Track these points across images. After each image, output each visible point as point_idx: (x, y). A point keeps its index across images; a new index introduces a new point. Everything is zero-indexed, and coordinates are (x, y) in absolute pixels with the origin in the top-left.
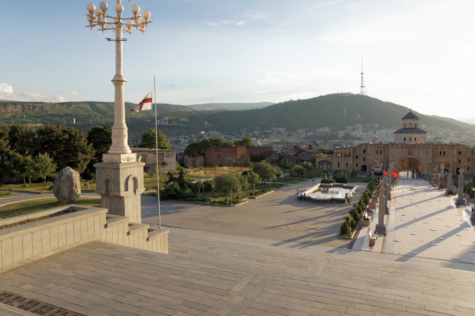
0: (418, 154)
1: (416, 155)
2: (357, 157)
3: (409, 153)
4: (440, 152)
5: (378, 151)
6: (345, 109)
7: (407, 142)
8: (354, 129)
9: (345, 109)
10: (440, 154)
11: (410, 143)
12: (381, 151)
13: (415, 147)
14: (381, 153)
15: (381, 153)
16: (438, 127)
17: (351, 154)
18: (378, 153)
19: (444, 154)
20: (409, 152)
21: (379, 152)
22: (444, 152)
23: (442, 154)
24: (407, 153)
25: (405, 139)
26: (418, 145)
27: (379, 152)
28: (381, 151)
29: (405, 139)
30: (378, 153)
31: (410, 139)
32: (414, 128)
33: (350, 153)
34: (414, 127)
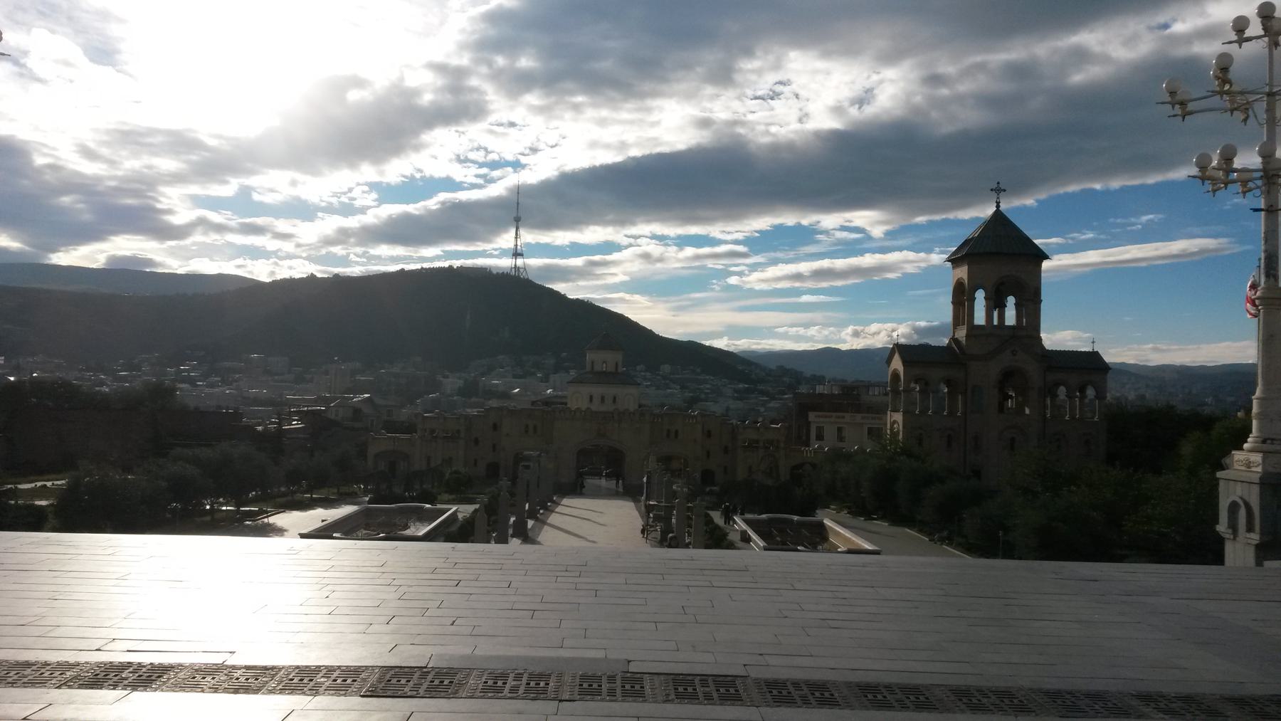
2: (476, 441)
4: (669, 431)
5: (527, 426)
10: (668, 436)
11: (603, 408)
16: (699, 370)
18: (527, 432)
22: (677, 432)
25: (591, 398)
28: (535, 428)
30: (527, 432)
31: (603, 399)
32: (610, 373)
33: (458, 431)
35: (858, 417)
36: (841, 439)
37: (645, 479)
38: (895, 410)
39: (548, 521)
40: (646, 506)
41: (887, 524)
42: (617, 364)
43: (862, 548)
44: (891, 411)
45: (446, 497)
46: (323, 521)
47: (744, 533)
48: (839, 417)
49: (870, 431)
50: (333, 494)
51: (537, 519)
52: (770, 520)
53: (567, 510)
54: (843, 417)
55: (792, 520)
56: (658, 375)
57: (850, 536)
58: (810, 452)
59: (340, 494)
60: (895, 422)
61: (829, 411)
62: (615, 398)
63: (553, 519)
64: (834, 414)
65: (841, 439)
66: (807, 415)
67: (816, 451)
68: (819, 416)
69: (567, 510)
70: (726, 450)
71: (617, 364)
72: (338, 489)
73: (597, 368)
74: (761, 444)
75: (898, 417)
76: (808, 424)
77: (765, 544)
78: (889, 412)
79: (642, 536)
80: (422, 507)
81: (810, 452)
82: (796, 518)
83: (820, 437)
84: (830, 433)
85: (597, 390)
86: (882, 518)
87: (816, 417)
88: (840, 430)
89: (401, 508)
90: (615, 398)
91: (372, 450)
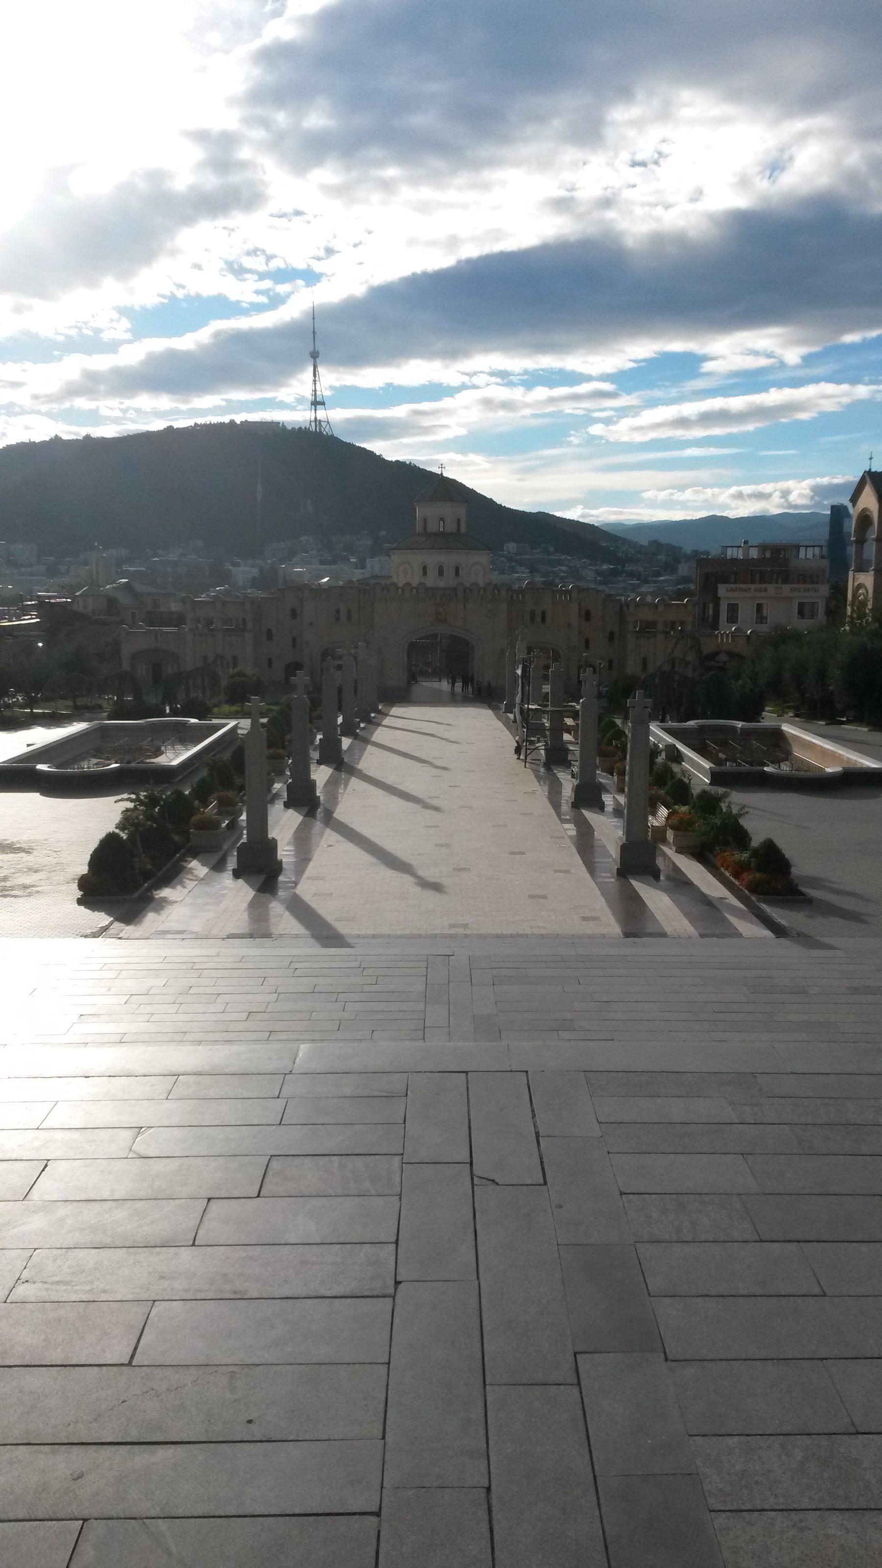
2: (269, 634)
4: (533, 614)
5: (338, 611)
7: (431, 581)
10: (532, 619)
11: (442, 584)
13: (456, 595)
14: (349, 618)
15: (349, 618)
16: (552, 549)
17: (250, 625)
19: (543, 620)
21: (343, 616)
22: (544, 613)
23: (538, 619)
25: (425, 568)
26: (465, 591)
27: (343, 616)
28: (349, 612)
29: (425, 568)
30: (338, 619)
32: (451, 534)
33: (244, 620)
34: (454, 531)
35: (786, 589)
36: (761, 618)
37: (519, 672)
38: (860, 569)
39: (373, 739)
40: (522, 711)
41: (865, 729)
42: (459, 520)
43: (859, 766)
44: (855, 571)
45: (226, 708)
46: (28, 745)
47: (671, 748)
48: (760, 590)
49: (801, 606)
50: (67, 707)
51: (355, 736)
52: (701, 729)
53: (399, 723)
54: (766, 590)
55: (734, 728)
56: (502, 556)
57: (832, 748)
58: (727, 636)
59: (77, 708)
60: (860, 586)
61: (745, 582)
62: (457, 569)
63: (380, 735)
64: (752, 586)
65: (761, 618)
66: (717, 588)
67: (734, 635)
68: (732, 590)
69: (399, 723)
70: (611, 637)
71: (459, 520)
72: (75, 702)
73: (432, 527)
74: (660, 627)
75: (867, 579)
76: (717, 601)
77: (713, 765)
78: (851, 574)
79: (516, 756)
80: (185, 724)
81: (727, 636)
82: (739, 724)
83: (732, 619)
84: (746, 612)
85: (433, 559)
86: (858, 720)
87: (727, 590)
88: (759, 607)
89: (154, 724)
90: (457, 569)
91: (127, 650)
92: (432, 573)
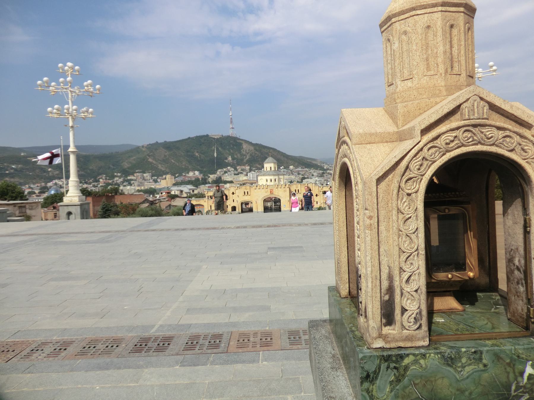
0: (278, 193)
1: (276, 194)
3: (271, 192)
5: (245, 192)
6: (215, 151)
7: (269, 183)
8: (226, 172)
9: (215, 151)
11: (272, 183)
12: (248, 192)
18: (245, 194)
20: (271, 192)
22: (298, 190)
24: (269, 193)
25: (267, 180)
28: (248, 192)
29: (267, 180)
92: (269, 181)
